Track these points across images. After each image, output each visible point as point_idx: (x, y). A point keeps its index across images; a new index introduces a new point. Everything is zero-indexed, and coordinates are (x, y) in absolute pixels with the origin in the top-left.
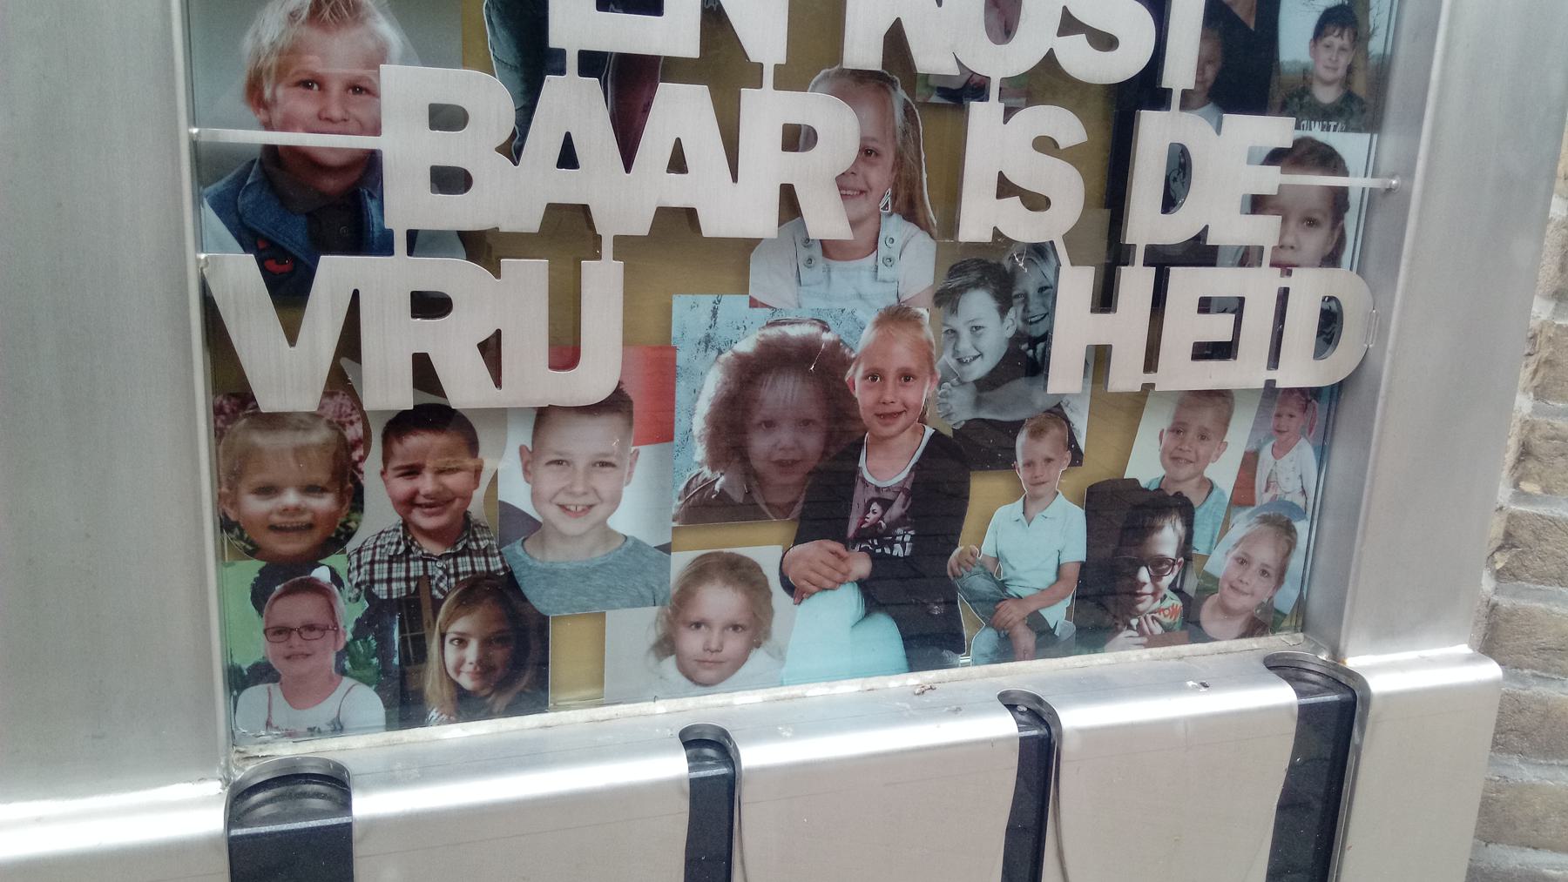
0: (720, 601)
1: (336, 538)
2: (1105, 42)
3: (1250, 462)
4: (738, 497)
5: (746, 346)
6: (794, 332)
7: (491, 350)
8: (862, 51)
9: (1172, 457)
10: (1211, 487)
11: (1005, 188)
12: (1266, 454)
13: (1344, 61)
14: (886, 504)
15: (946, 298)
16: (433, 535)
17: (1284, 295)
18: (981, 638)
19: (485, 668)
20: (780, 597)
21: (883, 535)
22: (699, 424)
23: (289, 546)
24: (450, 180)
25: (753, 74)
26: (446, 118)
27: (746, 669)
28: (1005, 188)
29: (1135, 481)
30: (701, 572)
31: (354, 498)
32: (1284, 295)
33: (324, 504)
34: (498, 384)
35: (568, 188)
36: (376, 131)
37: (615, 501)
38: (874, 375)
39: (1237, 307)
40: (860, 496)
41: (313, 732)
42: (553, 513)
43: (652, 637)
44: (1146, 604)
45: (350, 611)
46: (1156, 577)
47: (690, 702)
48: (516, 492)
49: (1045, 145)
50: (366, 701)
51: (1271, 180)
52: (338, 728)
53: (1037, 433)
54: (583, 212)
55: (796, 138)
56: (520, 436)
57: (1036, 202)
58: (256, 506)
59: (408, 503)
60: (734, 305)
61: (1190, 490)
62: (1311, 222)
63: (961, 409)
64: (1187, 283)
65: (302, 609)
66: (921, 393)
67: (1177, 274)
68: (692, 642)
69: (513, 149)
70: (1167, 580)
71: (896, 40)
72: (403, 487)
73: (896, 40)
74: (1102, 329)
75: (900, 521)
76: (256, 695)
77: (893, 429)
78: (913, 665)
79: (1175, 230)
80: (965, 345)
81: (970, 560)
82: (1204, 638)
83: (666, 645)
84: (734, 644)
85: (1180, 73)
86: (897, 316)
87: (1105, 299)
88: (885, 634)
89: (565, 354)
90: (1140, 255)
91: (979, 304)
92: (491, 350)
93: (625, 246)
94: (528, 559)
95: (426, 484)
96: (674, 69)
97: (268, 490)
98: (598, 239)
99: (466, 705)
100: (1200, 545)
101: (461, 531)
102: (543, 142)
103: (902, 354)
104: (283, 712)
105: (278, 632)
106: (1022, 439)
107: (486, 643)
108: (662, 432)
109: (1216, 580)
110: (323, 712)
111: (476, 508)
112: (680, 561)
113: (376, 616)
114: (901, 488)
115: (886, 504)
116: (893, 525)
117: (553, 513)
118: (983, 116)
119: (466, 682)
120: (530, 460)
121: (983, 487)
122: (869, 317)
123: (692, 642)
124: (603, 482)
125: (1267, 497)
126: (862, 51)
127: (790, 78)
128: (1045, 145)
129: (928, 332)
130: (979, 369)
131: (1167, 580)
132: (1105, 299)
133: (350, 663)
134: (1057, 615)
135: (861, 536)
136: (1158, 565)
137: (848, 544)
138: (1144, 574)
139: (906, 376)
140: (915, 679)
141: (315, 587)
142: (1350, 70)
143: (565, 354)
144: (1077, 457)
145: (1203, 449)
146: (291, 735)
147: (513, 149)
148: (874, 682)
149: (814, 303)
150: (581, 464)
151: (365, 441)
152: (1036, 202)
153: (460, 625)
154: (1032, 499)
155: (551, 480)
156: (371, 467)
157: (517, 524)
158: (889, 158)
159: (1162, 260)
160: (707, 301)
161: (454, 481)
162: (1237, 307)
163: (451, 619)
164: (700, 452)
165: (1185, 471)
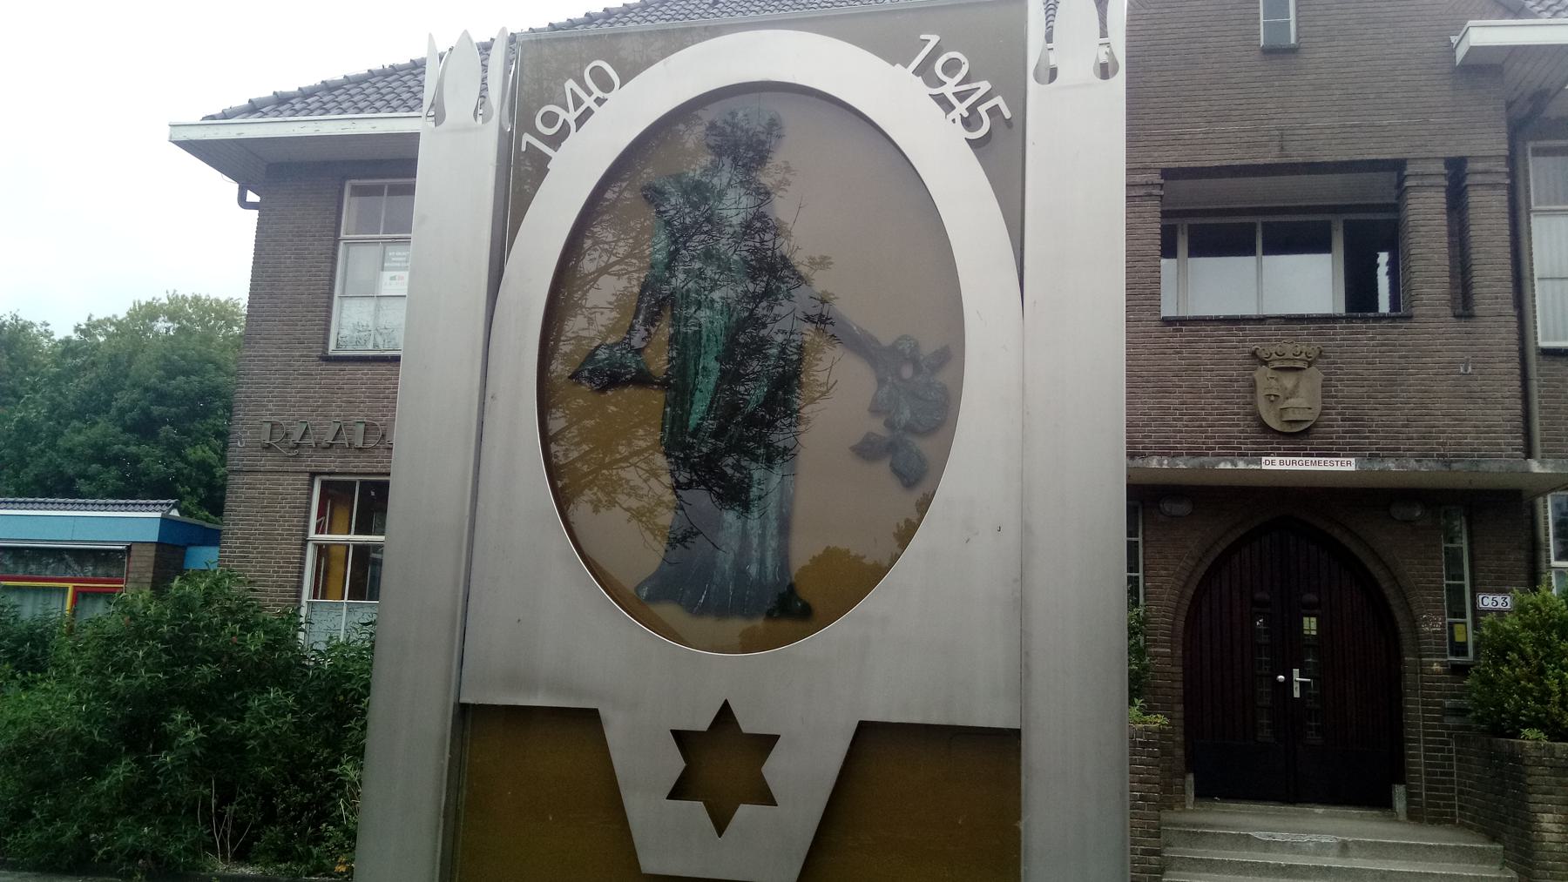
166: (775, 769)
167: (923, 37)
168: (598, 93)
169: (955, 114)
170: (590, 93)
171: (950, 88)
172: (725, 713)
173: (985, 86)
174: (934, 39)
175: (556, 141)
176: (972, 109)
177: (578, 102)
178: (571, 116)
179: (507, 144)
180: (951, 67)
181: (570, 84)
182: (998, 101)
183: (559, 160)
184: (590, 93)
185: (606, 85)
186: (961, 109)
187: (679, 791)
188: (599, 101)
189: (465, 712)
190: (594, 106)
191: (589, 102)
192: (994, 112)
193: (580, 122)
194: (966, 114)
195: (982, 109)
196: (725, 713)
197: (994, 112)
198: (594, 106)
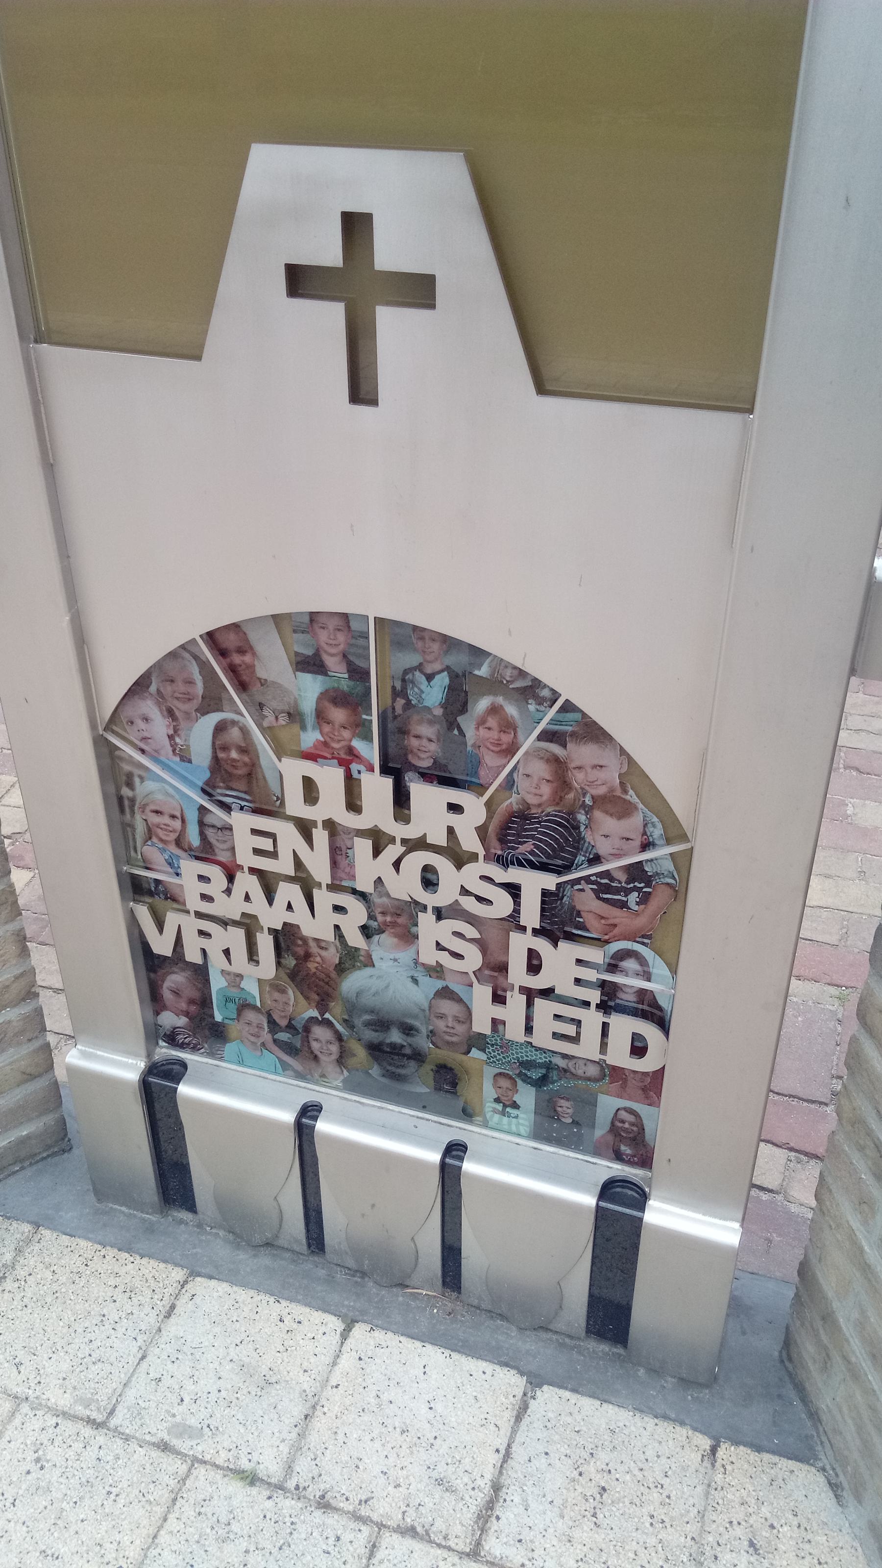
7: (227, 952)
17: (605, 1026)
24: (205, 897)
28: (439, 947)
32: (605, 1026)
34: (230, 964)
35: (249, 909)
39: (578, 1023)
54: (254, 917)
57: (458, 956)
67: (538, 1002)
74: (498, 1012)
79: (537, 982)
90: (517, 989)
92: (227, 952)
98: (262, 928)
118: (426, 920)
152: (458, 956)
159: (530, 995)
162: (578, 1023)
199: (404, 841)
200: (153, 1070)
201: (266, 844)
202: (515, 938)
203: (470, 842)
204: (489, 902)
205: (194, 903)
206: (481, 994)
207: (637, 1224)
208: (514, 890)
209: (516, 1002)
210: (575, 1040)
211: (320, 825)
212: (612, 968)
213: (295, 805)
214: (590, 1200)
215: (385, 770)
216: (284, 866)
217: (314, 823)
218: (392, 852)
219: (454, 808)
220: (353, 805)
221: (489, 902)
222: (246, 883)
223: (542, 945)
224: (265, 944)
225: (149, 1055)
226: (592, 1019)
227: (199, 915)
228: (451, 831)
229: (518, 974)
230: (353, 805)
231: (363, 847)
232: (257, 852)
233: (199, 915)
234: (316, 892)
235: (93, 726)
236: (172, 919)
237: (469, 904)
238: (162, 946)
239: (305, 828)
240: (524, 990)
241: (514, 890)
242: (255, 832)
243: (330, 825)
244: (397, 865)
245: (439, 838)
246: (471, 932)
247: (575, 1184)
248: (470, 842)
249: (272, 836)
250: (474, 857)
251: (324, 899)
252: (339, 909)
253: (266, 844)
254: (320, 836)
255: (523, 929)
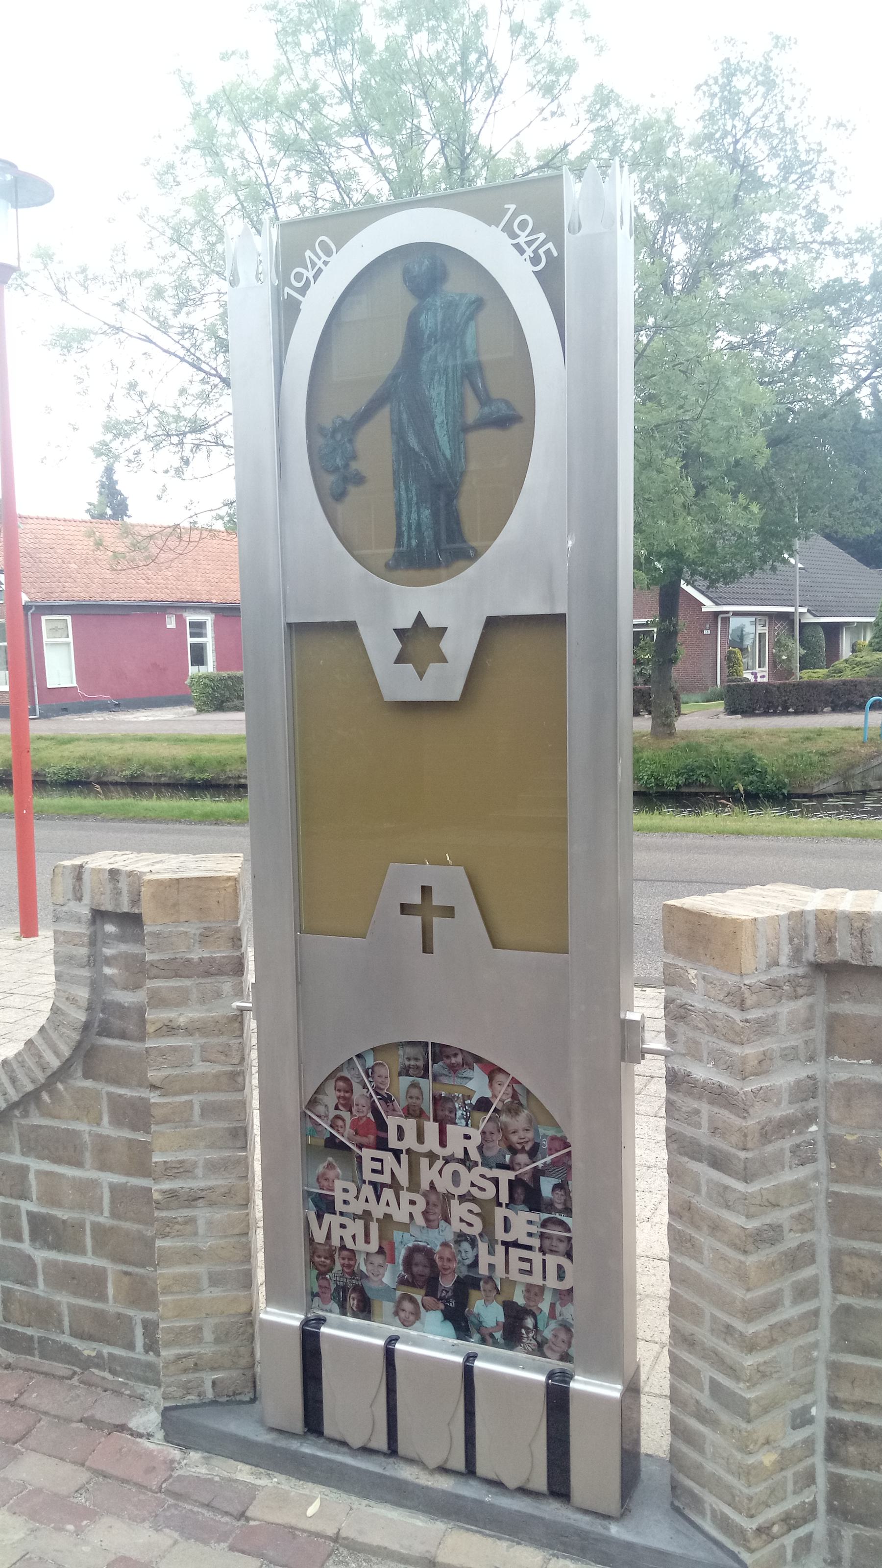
0: (407, 1305)
1: (331, 1270)
2: (482, 1189)
3: (553, 1306)
4: (410, 1280)
5: (410, 1245)
6: (421, 1244)
7: (354, 1237)
8: (425, 1186)
9: (527, 1298)
10: (541, 1311)
11: (462, 1220)
12: (558, 1305)
13: (563, 1198)
14: (447, 1292)
15: (458, 1242)
16: (347, 1273)
17: (544, 1261)
18: (476, 1336)
19: (358, 1307)
20: (422, 1308)
21: (448, 1301)
22: (401, 1262)
23: (322, 1269)
24: (345, 1202)
25: (402, 1188)
26: (345, 1190)
27: (415, 1325)
28: (462, 1220)
29: (516, 1303)
30: (405, 1297)
31: (333, 1261)
32: (544, 1261)
33: (328, 1262)
35: (367, 1207)
36: (333, 1190)
37: (383, 1275)
38: (441, 1258)
40: (440, 1289)
41: (327, 1311)
42: (371, 1275)
43: (393, 1310)
44: (525, 1340)
45: (333, 1286)
46: (528, 1333)
47: (400, 1329)
48: (363, 1268)
49: (470, 1211)
50: (335, 1307)
51: (534, 1229)
52: (331, 1311)
53: (486, 1283)
55: (412, 1202)
56: (363, 1256)
57: (470, 1225)
58: (317, 1259)
59: (343, 1265)
60: (407, 1235)
61: (534, 1309)
62: (561, 1241)
63: (464, 1272)
64: (514, 1252)
65: (324, 1283)
66: (454, 1265)
68: (402, 1314)
69: (357, 1198)
70: (531, 1335)
71: (432, 1186)
72: (342, 1262)
73: (432, 1186)
75: (451, 1297)
76: (316, 1299)
77: (446, 1273)
78: (458, 1339)
79: (509, 1238)
80: (463, 1254)
81: (471, 1313)
82: (544, 1355)
83: (396, 1313)
84: (412, 1318)
85: (504, 1198)
86: (445, 1244)
87: (491, 1252)
88: (449, 1328)
89: (367, 1241)
90: (500, 1242)
91: (466, 1246)
92: (354, 1237)
93: (378, 1220)
94: (367, 1285)
95: (346, 1262)
96: (384, 1185)
97: (319, 1257)
99: (355, 1315)
100: (540, 1326)
101: (353, 1274)
102: (362, 1197)
103: (447, 1254)
104: (322, 1305)
105: (320, 1286)
106: (482, 1283)
107: (358, 1301)
108: (393, 1261)
109: (547, 1339)
110: (328, 1307)
111: (356, 1269)
112: (398, 1293)
113: (337, 1288)
114: (450, 1288)
115: (447, 1292)
116: (449, 1298)
117: (371, 1275)
118: (454, 1203)
119: (355, 1309)
120: (366, 1261)
121: (473, 1293)
122: (439, 1244)
123: (402, 1314)
124: (381, 1270)
125: (560, 1318)
126: (425, 1186)
127: (409, 1190)
128: (470, 1211)
129: (453, 1250)
130: (468, 1262)
131: (531, 1335)
132: (491, 1252)
133: (334, 1298)
134: (498, 1335)
135: (441, 1299)
136: (527, 1329)
137: (439, 1300)
138: (523, 1331)
139: (449, 1260)
140: (456, 1341)
141: (326, 1279)
142: (565, 1200)
143: (367, 1241)
144: (498, 1292)
145: (537, 1298)
146: (322, 1310)
147: (357, 1198)
148: (446, 1339)
149: (424, 1238)
150: (376, 1265)
151: (335, 1250)
152: (470, 1225)
153: (353, 1295)
154: (487, 1302)
155: (370, 1267)
156: (336, 1256)
157: (363, 1276)
158: (440, 1207)
159: (507, 1245)
160: (401, 1233)
161: (351, 1263)
163: (352, 1293)
164: (401, 1268)
165: (532, 1304)
166: (446, 645)
167: (506, 206)
168: (324, 258)
169: (526, 256)
170: (320, 258)
171: (522, 240)
172: (420, 618)
173: (542, 236)
174: (513, 207)
175: (303, 291)
176: (535, 251)
177: (314, 264)
178: (310, 274)
179: (277, 291)
180: (523, 225)
181: (308, 253)
182: (550, 245)
183: (306, 303)
184: (320, 258)
185: (329, 253)
186: (529, 252)
187: (400, 660)
188: (326, 263)
189: (289, 625)
190: (323, 267)
191: (320, 264)
192: (548, 252)
193: (316, 277)
194: (532, 255)
195: (541, 251)
196: (420, 618)
197: (548, 252)
198: (323, 267)
199: (444, 1158)
200: (306, 1322)
201: (377, 1166)
202: (497, 1209)
203: (475, 1155)
204: (484, 1190)
205: (339, 1206)
206: (483, 1247)
207: (568, 1389)
208: (496, 1181)
209: (500, 1249)
210: (530, 1272)
211: (404, 1152)
212: (544, 1224)
213: (393, 1143)
214: (542, 1378)
215: (435, 1120)
216: (386, 1178)
217: (401, 1151)
218: (439, 1163)
219: (467, 1137)
220: (420, 1138)
221: (484, 1190)
222: (368, 1190)
223: (509, 1213)
224: (374, 1228)
225: (307, 1314)
226: (536, 1257)
227: (342, 1214)
228: (465, 1149)
229: (500, 1235)
230: (420, 1138)
231: (424, 1162)
232: (374, 1171)
233: (342, 1214)
234: (401, 1192)
235: (301, 1108)
236: (327, 1217)
237: (475, 1192)
238: (320, 1236)
239: (397, 1153)
240: (504, 1243)
241: (496, 1181)
242: (373, 1159)
243: (408, 1151)
244: (440, 1172)
245: (460, 1155)
246: (476, 1209)
247: (538, 1370)
248: (475, 1155)
249: (381, 1161)
250: (476, 1164)
251: (405, 1196)
252: (412, 1202)
253: (377, 1166)
254: (404, 1158)
255: (500, 1205)
